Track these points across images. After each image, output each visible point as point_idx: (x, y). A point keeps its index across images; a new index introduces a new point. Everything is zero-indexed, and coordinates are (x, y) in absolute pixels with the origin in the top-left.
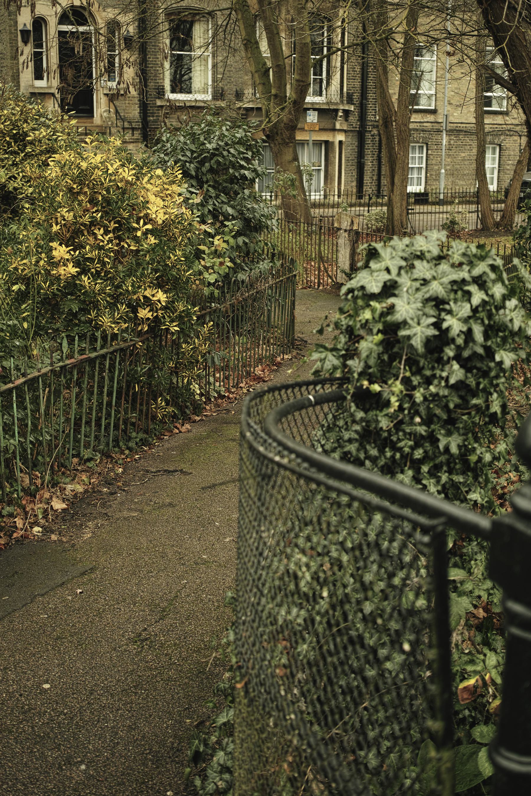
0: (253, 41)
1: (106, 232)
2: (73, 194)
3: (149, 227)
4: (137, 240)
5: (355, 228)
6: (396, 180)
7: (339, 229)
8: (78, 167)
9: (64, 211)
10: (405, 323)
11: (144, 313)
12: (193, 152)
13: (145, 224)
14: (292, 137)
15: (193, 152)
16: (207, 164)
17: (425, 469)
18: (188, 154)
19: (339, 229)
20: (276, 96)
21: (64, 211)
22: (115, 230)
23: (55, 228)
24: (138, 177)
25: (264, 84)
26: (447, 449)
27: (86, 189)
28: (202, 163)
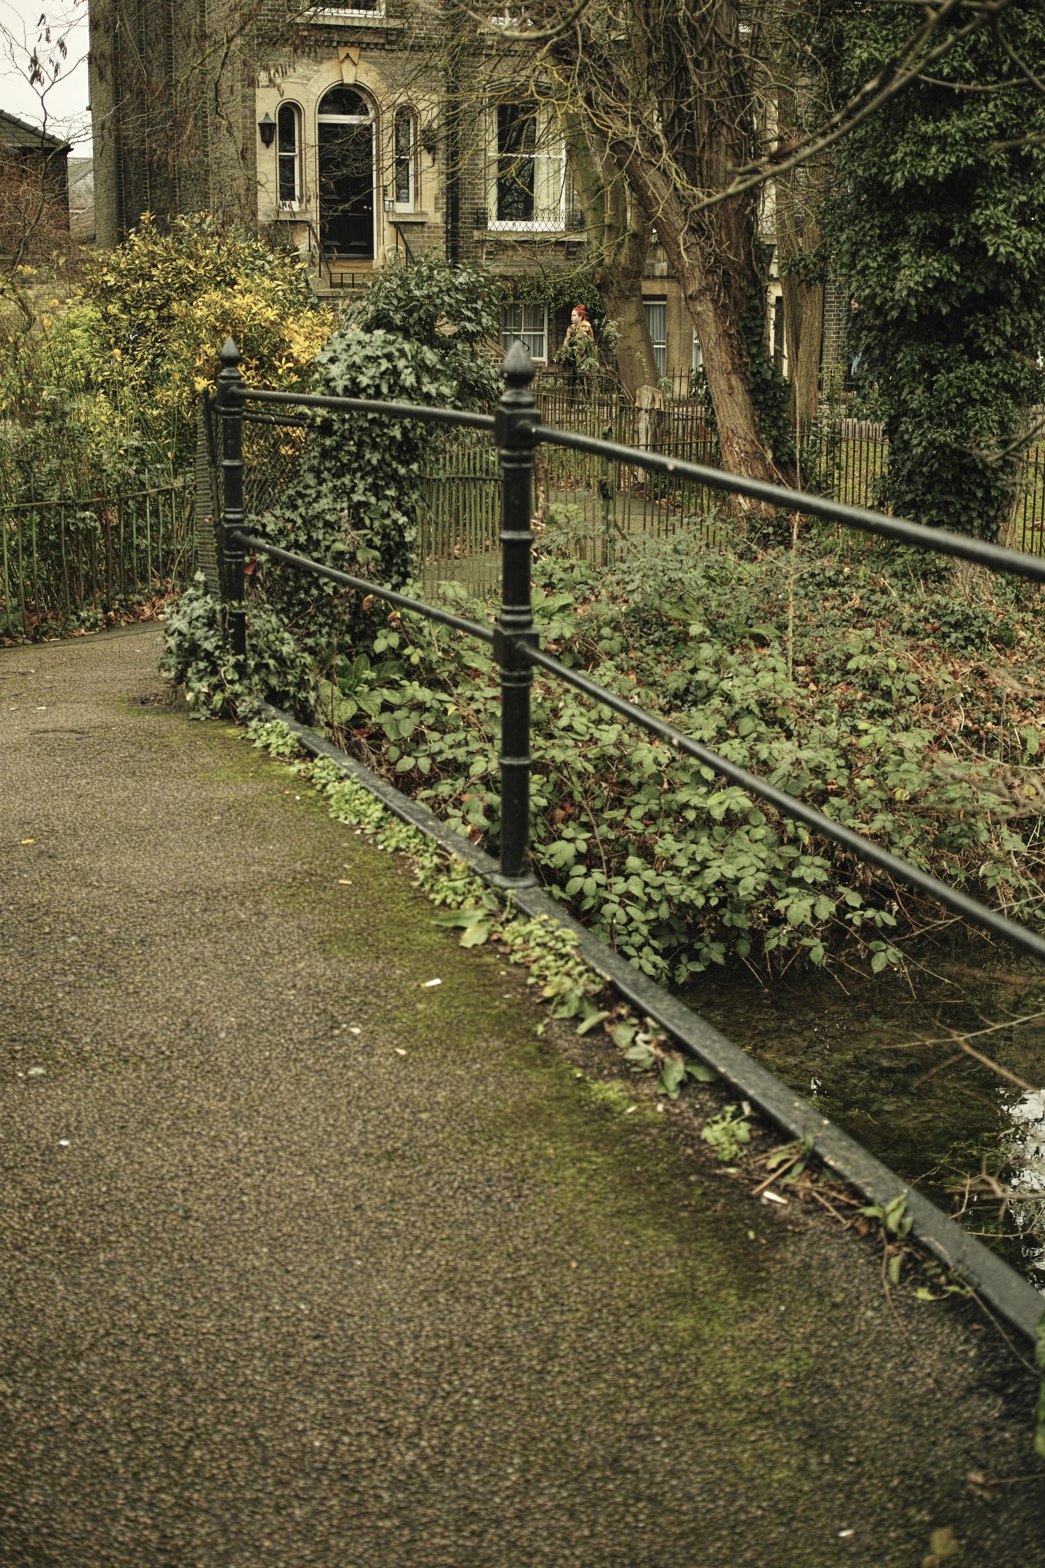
0: (580, 146)
1: (248, 369)
2: (216, 332)
3: (291, 365)
4: (280, 379)
5: (657, 406)
6: (801, 354)
7: (640, 409)
8: (222, 306)
9: (206, 347)
10: (333, 379)
11: (285, 450)
12: (399, 300)
13: (287, 362)
14: (635, 289)
15: (399, 300)
16: (415, 315)
17: (359, 475)
18: (395, 302)
19: (640, 409)
20: (610, 227)
21: (206, 347)
22: (257, 368)
23: (198, 363)
24: (282, 317)
25: (595, 209)
26: (369, 461)
27: (229, 328)
28: (410, 312)
